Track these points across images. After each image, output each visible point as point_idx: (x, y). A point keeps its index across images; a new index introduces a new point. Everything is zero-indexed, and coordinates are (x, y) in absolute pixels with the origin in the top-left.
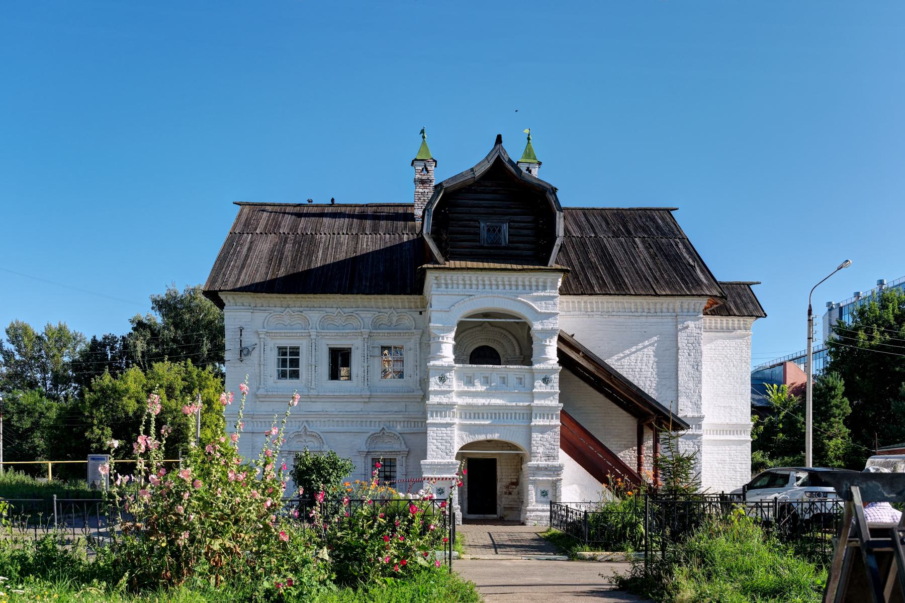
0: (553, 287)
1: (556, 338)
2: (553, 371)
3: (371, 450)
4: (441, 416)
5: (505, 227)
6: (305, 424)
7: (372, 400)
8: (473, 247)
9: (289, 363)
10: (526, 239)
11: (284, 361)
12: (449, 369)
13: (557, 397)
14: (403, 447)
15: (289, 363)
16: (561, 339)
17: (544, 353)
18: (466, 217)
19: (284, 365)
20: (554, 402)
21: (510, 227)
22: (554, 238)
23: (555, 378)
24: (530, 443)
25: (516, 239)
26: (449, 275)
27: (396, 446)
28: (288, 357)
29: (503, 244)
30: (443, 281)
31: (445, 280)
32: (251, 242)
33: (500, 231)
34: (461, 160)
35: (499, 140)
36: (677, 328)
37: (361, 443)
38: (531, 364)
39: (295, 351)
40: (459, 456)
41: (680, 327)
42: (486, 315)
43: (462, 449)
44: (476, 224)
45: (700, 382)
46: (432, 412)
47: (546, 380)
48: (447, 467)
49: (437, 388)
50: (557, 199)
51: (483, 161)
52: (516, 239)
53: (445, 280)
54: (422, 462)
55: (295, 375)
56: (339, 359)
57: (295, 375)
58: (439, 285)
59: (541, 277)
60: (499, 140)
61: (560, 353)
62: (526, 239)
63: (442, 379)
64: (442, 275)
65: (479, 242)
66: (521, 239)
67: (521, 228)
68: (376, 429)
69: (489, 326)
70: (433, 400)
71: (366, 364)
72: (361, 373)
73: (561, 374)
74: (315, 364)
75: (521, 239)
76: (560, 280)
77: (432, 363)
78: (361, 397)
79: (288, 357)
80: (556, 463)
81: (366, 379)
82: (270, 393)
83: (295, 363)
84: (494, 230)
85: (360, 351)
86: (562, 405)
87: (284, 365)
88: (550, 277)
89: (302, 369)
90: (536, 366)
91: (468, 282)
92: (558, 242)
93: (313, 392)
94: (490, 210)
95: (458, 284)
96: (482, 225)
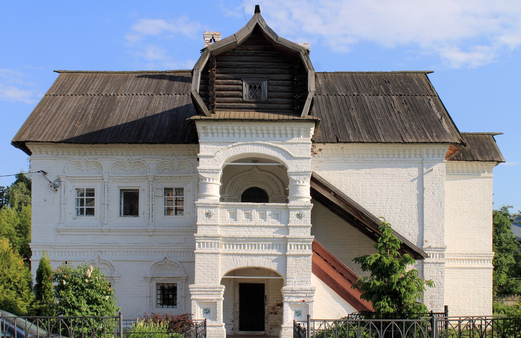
0: (307, 135)
1: (309, 179)
2: (306, 208)
4: (207, 247)
5: (265, 84)
6: (99, 254)
7: (155, 233)
8: (237, 102)
9: (86, 203)
10: (283, 94)
11: (82, 201)
12: (215, 206)
13: (309, 230)
15: (86, 203)
16: (314, 180)
17: (297, 192)
19: (82, 204)
20: (306, 234)
21: (269, 84)
22: (306, 92)
23: (308, 214)
24: (286, 270)
25: (273, 94)
26: (215, 126)
27: (177, 274)
28: (85, 197)
29: (263, 99)
30: (209, 131)
31: (212, 129)
32: (62, 103)
33: (260, 88)
34: (231, 27)
35: (257, 9)
36: (423, 170)
38: (287, 201)
39: (91, 193)
40: (224, 281)
41: (425, 170)
42: (255, 160)
45: (443, 217)
46: (199, 243)
47: (299, 216)
48: (213, 290)
49: (204, 223)
50: (309, 59)
51: (244, 28)
52: (273, 94)
53: (212, 129)
54: (190, 286)
55: (91, 212)
57: (91, 212)
58: (206, 134)
59: (296, 126)
60: (257, 9)
61: (313, 192)
62: (283, 94)
63: (208, 215)
65: (242, 97)
66: (279, 94)
68: (160, 257)
69: (255, 167)
70: (201, 232)
71: (151, 203)
74: (109, 203)
75: (279, 94)
76: (313, 129)
77: (200, 201)
79: (85, 197)
80: (308, 287)
82: (68, 228)
83: (91, 201)
84: (255, 87)
86: (313, 237)
87: (82, 204)
88: (303, 126)
89: (97, 207)
90: (291, 203)
91: (231, 131)
92: (310, 96)
93: (106, 227)
94: (252, 70)
95: (222, 133)
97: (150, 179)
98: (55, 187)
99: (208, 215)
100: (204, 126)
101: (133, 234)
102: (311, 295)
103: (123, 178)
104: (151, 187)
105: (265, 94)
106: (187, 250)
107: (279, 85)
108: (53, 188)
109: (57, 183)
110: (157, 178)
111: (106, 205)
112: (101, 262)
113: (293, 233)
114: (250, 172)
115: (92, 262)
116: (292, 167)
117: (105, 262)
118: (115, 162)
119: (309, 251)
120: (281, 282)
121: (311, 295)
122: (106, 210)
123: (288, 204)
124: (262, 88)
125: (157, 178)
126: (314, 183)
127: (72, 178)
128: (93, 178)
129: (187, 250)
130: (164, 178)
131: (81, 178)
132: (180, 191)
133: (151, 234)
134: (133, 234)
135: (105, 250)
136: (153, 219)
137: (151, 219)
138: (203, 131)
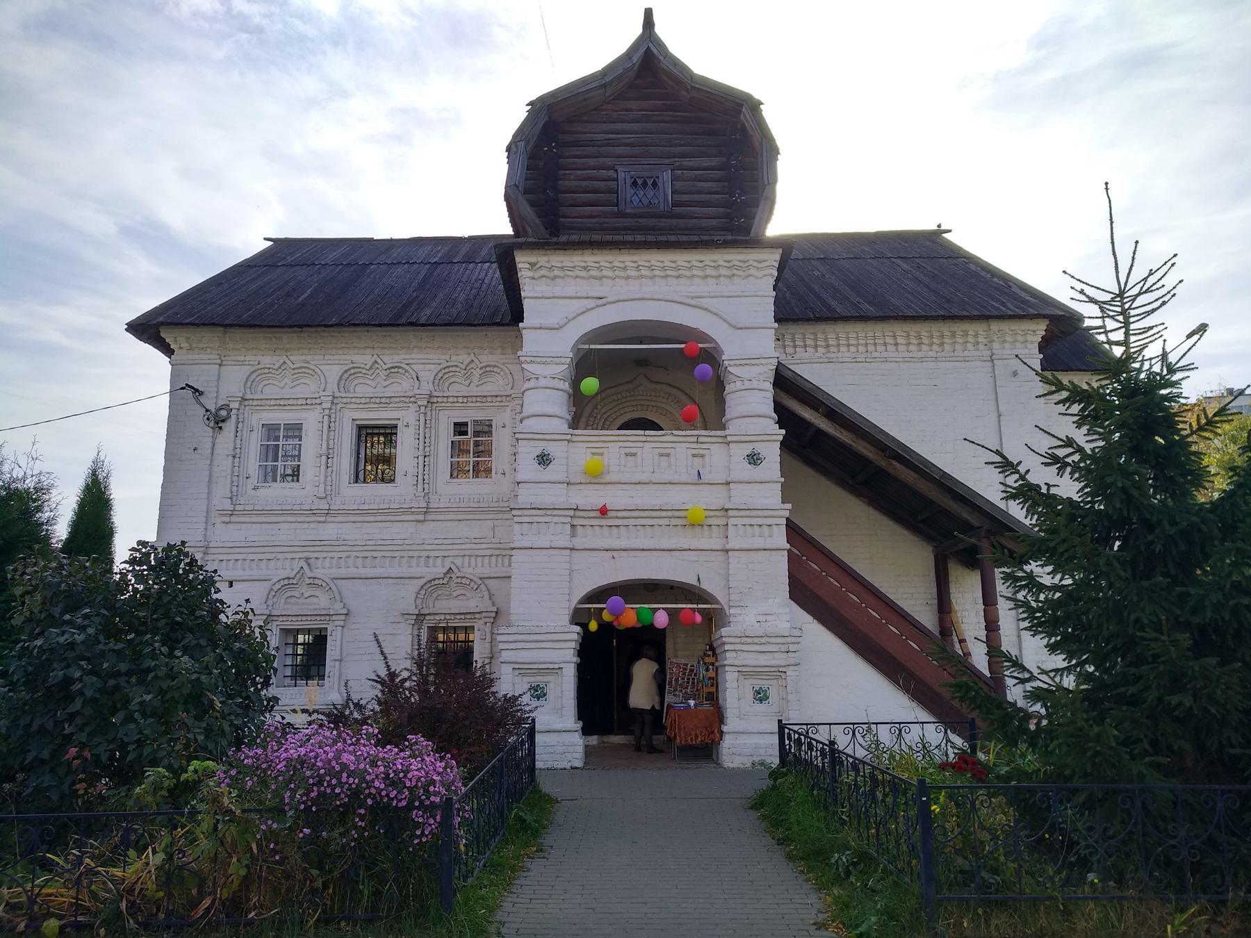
3: (425, 611)
5: (667, 176)
6: (303, 563)
7: (429, 517)
14: (485, 605)
18: (591, 162)
25: (686, 197)
33: (655, 184)
37: (406, 597)
43: (581, 602)
44: (611, 173)
47: (754, 459)
56: (374, 449)
61: (779, 408)
63: (544, 459)
64: (541, 259)
67: (697, 179)
72: (412, 471)
73: (785, 445)
78: (409, 511)
81: (423, 479)
84: (645, 184)
85: (412, 430)
94: (637, 150)
96: (621, 175)
97: (420, 403)
98: (217, 420)
99: (544, 459)
100: (533, 259)
101: (379, 518)
102: (792, 648)
103: (363, 401)
104: (422, 419)
105: (666, 199)
106: (497, 552)
107: (697, 179)
108: (212, 424)
109: (224, 413)
110: (435, 400)
111: (324, 458)
112: (308, 581)
113: (741, 496)
114: (630, 386)
115: (286, 582)
116: (731, 348)
117: (316, 581)
118: (347, 367)
119: (779, 538)
120: (713, 618)
121: (792, 648)
122: (323, 467)
123: (727, 432)
124: (660, 184)
125: (435, 400)
126: (782, 394)
127: (255, 403)
128: (300, 402)
129: (497, 552)
130: (451, 399)
131: (273, 402)
132: (484, 429)
133: (421, 517)
134: (379, 518)
135: (316, 555)
136: (426, 486)
137: (420, 486)
138: (530, 274)
